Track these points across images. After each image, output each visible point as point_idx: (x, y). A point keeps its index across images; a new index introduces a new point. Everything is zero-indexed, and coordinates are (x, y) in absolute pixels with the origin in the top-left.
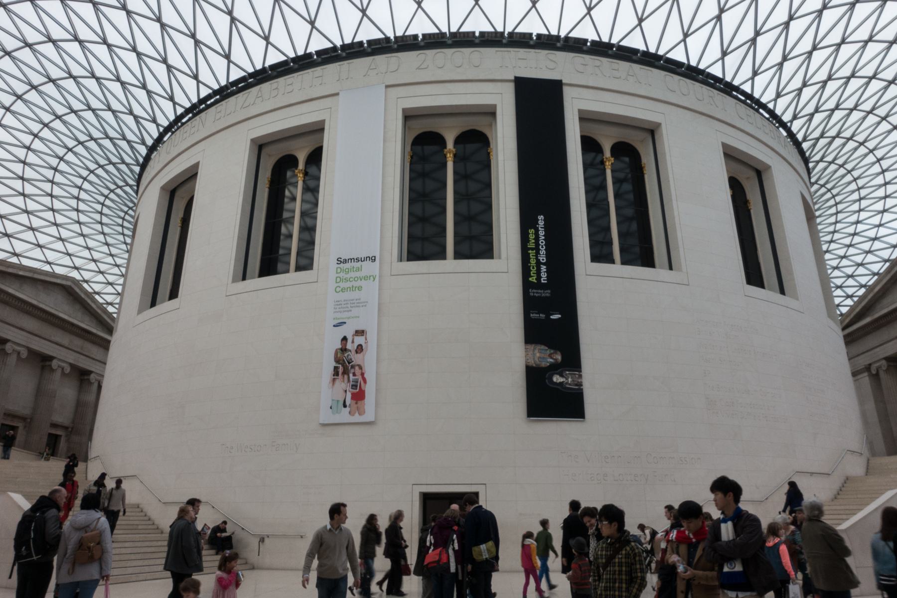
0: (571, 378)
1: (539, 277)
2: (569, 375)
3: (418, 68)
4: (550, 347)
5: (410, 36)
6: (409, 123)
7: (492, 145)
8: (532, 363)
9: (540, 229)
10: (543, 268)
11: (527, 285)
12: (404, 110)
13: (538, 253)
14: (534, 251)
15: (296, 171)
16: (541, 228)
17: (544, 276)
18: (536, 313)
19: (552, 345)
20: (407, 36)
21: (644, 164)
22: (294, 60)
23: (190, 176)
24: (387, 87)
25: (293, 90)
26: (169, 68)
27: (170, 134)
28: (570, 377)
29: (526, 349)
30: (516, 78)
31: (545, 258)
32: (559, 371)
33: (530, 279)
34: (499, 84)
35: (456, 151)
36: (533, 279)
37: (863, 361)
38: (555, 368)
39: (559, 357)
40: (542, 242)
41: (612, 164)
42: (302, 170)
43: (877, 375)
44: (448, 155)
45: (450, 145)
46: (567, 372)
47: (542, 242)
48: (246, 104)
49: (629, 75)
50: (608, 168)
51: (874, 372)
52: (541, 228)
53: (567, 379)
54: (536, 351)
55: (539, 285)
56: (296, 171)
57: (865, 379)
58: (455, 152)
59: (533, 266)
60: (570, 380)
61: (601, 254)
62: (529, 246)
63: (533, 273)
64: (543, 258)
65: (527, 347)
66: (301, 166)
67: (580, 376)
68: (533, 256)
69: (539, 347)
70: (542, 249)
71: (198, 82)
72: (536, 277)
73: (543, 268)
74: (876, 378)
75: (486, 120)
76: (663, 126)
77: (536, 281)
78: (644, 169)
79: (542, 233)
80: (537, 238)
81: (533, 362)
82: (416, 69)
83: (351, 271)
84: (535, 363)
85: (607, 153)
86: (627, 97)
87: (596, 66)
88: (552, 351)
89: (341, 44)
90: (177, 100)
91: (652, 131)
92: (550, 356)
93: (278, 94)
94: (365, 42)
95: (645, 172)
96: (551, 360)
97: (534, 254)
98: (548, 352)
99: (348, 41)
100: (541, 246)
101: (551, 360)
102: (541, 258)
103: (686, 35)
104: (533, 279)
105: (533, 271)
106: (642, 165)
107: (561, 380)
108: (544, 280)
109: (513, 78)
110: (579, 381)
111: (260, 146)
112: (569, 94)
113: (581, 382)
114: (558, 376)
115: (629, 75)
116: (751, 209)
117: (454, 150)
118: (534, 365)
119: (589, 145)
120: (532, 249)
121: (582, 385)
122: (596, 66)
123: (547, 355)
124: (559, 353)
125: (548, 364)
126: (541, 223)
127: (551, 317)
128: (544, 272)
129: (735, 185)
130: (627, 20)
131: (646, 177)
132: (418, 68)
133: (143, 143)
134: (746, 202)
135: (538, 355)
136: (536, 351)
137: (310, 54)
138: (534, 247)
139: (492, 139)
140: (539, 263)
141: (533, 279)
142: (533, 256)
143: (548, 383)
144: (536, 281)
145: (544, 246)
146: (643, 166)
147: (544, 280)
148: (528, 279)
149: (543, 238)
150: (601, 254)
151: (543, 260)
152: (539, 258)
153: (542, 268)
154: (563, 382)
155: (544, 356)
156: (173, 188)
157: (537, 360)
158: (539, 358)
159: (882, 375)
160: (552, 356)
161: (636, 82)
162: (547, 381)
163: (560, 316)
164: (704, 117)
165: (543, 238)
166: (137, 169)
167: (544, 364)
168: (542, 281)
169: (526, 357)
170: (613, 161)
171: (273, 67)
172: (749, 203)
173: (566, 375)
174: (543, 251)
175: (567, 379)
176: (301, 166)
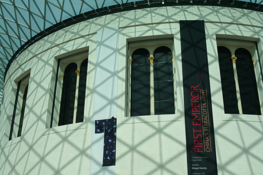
5: (130, 3)
20: (128, 3)
22: (74, 18)
23: (27, 75)
26: (30, 13)
27: (18, 54)
56: (76, 71)
66: (78, 69)
75: (169, 42)
89: (97, 9)
90: (32, 29)
94: (108, 7)
99: (100, 7)
111: (59, 60)
133: (7, 59)
137: (82, 14)
156: (20, 80)
166: (4, 70)
171: (65, 21)
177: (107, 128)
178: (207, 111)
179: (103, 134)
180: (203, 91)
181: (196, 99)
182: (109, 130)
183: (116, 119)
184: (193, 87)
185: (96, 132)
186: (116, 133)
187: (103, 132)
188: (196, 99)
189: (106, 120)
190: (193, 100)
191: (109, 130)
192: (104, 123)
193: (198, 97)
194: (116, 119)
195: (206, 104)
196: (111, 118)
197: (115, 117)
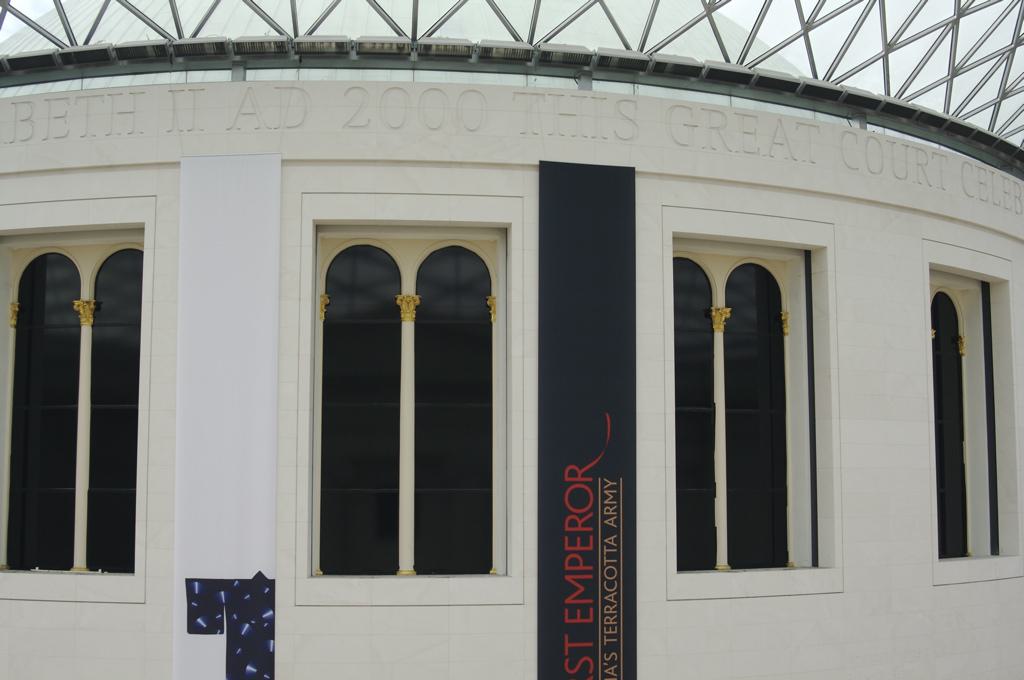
7: (497, 290)
12: (314, 221)
15: (76, 303)
21: (787, 313)
24: (284, 162)
25: (68, 132)
34: (518, 173)
44: (404, 307)
45: (409, 286)
50: (719, 328)
58: (418, 302)
61: (694, 554)
76: (830, 253)
78: (784, 326)
85: (719, 298)
93: (31, 137)
95: (786, 330)
103: (889, 47)
106: (781, 315)
117: (417, 297)
119: (689, 278)
129: (943, 312)
130: (782, 23)
131: (787, 339)
134: (956, 339)
139: (497, 276)
146: (783, 318)
150: (694, 554)
161: (786, 158)
164: (905, 215)
170: (728, 316)
176: (87, 292)
177: (235, 616)
178: (617, 565)
179: (217, 643)
180: (611, 483)
181: (583, 520)
182: (247, 626)
183: (274, 581)
184: (577, 468)
185: (193, 628)
186: (274, 639)
187: (222, 633)
188: (583, 520)
189: (233, 581)
190: (573, 523)
191: (247, 626)
192: (222, 593)
193: (589, 512)
194: (272, 583)
195: (617, 541)
196: (250, 576)
197: (269, 576)
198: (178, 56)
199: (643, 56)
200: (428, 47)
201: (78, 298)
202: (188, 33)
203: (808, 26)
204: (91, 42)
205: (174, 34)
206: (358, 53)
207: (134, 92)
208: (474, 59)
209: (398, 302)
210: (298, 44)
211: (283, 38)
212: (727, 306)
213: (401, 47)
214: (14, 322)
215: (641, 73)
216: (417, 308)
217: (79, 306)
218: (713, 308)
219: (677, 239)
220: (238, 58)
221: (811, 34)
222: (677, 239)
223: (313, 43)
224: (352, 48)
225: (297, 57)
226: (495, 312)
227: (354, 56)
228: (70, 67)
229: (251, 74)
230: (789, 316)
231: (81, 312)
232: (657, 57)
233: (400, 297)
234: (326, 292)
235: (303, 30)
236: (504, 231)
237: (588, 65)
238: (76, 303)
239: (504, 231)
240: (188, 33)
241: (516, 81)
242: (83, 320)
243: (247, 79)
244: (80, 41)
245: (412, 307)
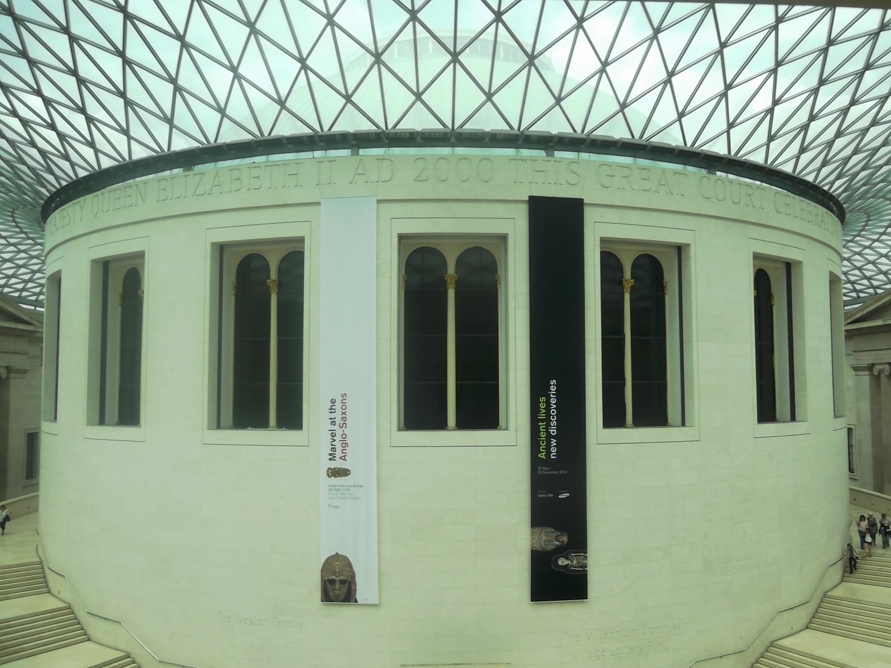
0: (576, 560)
1: (548, 452)
2: (574, 557)
3: (416, 180)
4: (557, 529)
6: (403, 241)
7: (501, 271)
8: (538, 547)
9: (552, 396)
10: (554, 442)
11: (535, 462)
13: (548, 425)
14: (545, 423)
15: (268, 281)
16: (553, 394)
17: (554, 450)
18: (544, 494)
19: (559, 527)
24: (379, 201)
28: (575, 559)
29: (532, 533)
30: (530, 197)
31: (555, 431)
32: (565, 553)
33: (539, 455)
34: (512, 206)
35: (458, 277)
36: (542, 456)
37: (866, 359)
38: (561, 551)
39: (565, 539)
40: (553, 412)
41: (631, 286)
42: (274, 281)
43: (878, 377)
44: (449, 281)
46: (573, 554)
47: (553, 412)
48: (200, 191)
49: (660, 185)
50: (627, 291)
51: (876, 374)
52: (553, 394)
53: (572, 562)
54: (543, 534)
55: (548, 462)
57: (866, 378)
58: (456, 279)
59: (543, 440)
60: (575, 562)
62: (539, 418)
63: (543, 449)
64: (553, 431)
65: (534, 531)
67: (586, 558)
68: (543, 428)
69: (546, 530)
70: (552, 419)
71: (130, 138)
72: (545, 453)
73: (554, 442)
74: (876, 379)
77: (545, 458)
78: (665, 289)
79: (553, 401)
80: (548, 408)
81: (539, 546)
82: (414, 180)
83: (346, 441)
84: (542, 549)
85: (628, 274)
86: (655, 214)
87: (623, 177)
88: (559, 534)
91: (680, 250)
92: (557, 539)
95: (666, 292)
96: (557, 543)
97: (545, 427)
98: (555, 534)
100: (552, 416)
101: (557, 543)
102: (552, 431)
103: (731, 125)
104: (542, 455)
105: (543, 445)
106: (663, 283)
107: (567, 562)
108: (553, 456)
109: (527, 199)
110: (584, 562)
112: (590, 217)
113: (586, 564)
114: (564, 559)
115: (660, 185)
116: (773, 305)
117: (456, 275)
118: (540, 549)
119: (609, 262)
120: (542, 420)
121: (586, 567)
122: (623, 177)
123: (554, 537)
124: (566, 534)
125: (554, 547)
126: (553, 389)
127: (560, 497)
128: (554, 446)
129: (762, 280)
131: (667, 297)
132: (416, 180)
134: (769, 296)
135: (544, 538)
136: (543, 534)
138: (544, 418)
140: (549, 437)
141: (542, 456)
142: (543, 428)
143: (553, 567)
144: (545, 458)
145: (555, 416)
146: (665, 285)
147: (553, 456)
148: (537, 455)
149: (555, 406)
151: (553, 432)
152: (550, 430)
153: (552, 442)
154: (568, 564)
155: (550, 539)
157: (543, 544)
158: (546, 541)
159: (884, 380)
160: (559, 538)
162: (552, 565)
163: (568, 494)
164: (738, 225)
165: (555, 406)
167: (550, 547)
168: (552, 457)
169: (532, 541)
170: (633, 284)
172: (773, 298)
173: (571, 557)
174: (554, 423)
175: (572, 561)
176: (273, 275)
198: (321, 141)
199: (583, 136)
200: (461, 134)
201: (269, 278)
202: (326, 128)
203: (681, 115)
204: (272, 134)
205: (319, 129)
206: (422, 138)
207: (298, 163)
208: (487, 140)
209: (445, 278)
210: (388, 133)
211: (380, 131)
212: (632, 279)
213: (445, 134)
214: (234, 292)
215: (583, 146)
216: (456, 282)
217: (269, 283)
218: (624, 280)
219: (603, 241)
220: (354, 142)
221: (683, 120)
222: (603, 241)
223: (396, 133)
224: (418, 135)
225: (387, 141)
226: (499, 283)
227: (419, 140)
228: (261, 149)
229: (362, 152)
230: (668, 283)
231: (271, 286)
232: (591, 136)
233: (447, 276)
234: (406, 273)
235: (390, 127)
236: (504, 238)
237: (552, 142)
238: (268, 281)
239: (504, 238)
240: (326, 128)
241: (510, 152)
242: (272, 291)
243: (360, 154)
244: (266, 134)
245: (454, 281)
